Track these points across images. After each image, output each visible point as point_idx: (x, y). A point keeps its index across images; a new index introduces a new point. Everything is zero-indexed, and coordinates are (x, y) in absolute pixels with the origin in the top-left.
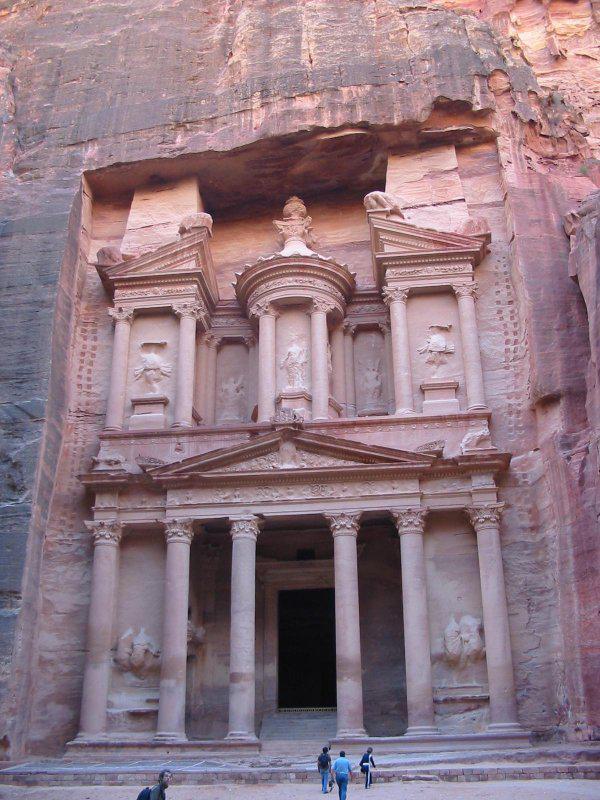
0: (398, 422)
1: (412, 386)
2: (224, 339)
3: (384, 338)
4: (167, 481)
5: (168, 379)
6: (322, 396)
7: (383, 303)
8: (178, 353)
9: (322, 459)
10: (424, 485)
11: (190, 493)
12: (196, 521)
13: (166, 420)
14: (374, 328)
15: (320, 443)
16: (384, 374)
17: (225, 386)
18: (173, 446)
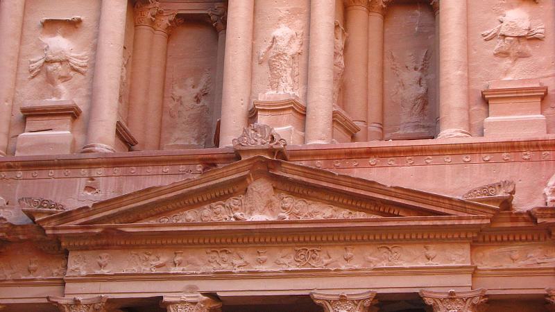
0: (442, 150)
1: (469, 94)
2: (178, 16)
3: (435, 17)
4: (69, 237)
5: (82, 77)
6: (322, 106)
8: (97, 36)
9: (314, 207)
10: (481, 254)
11: (104, 256)
12: (110, 301)
13: (74, 141)
15: (311, 181)
16: (431, 77)
17: (178, 92)
18: (83, 182)
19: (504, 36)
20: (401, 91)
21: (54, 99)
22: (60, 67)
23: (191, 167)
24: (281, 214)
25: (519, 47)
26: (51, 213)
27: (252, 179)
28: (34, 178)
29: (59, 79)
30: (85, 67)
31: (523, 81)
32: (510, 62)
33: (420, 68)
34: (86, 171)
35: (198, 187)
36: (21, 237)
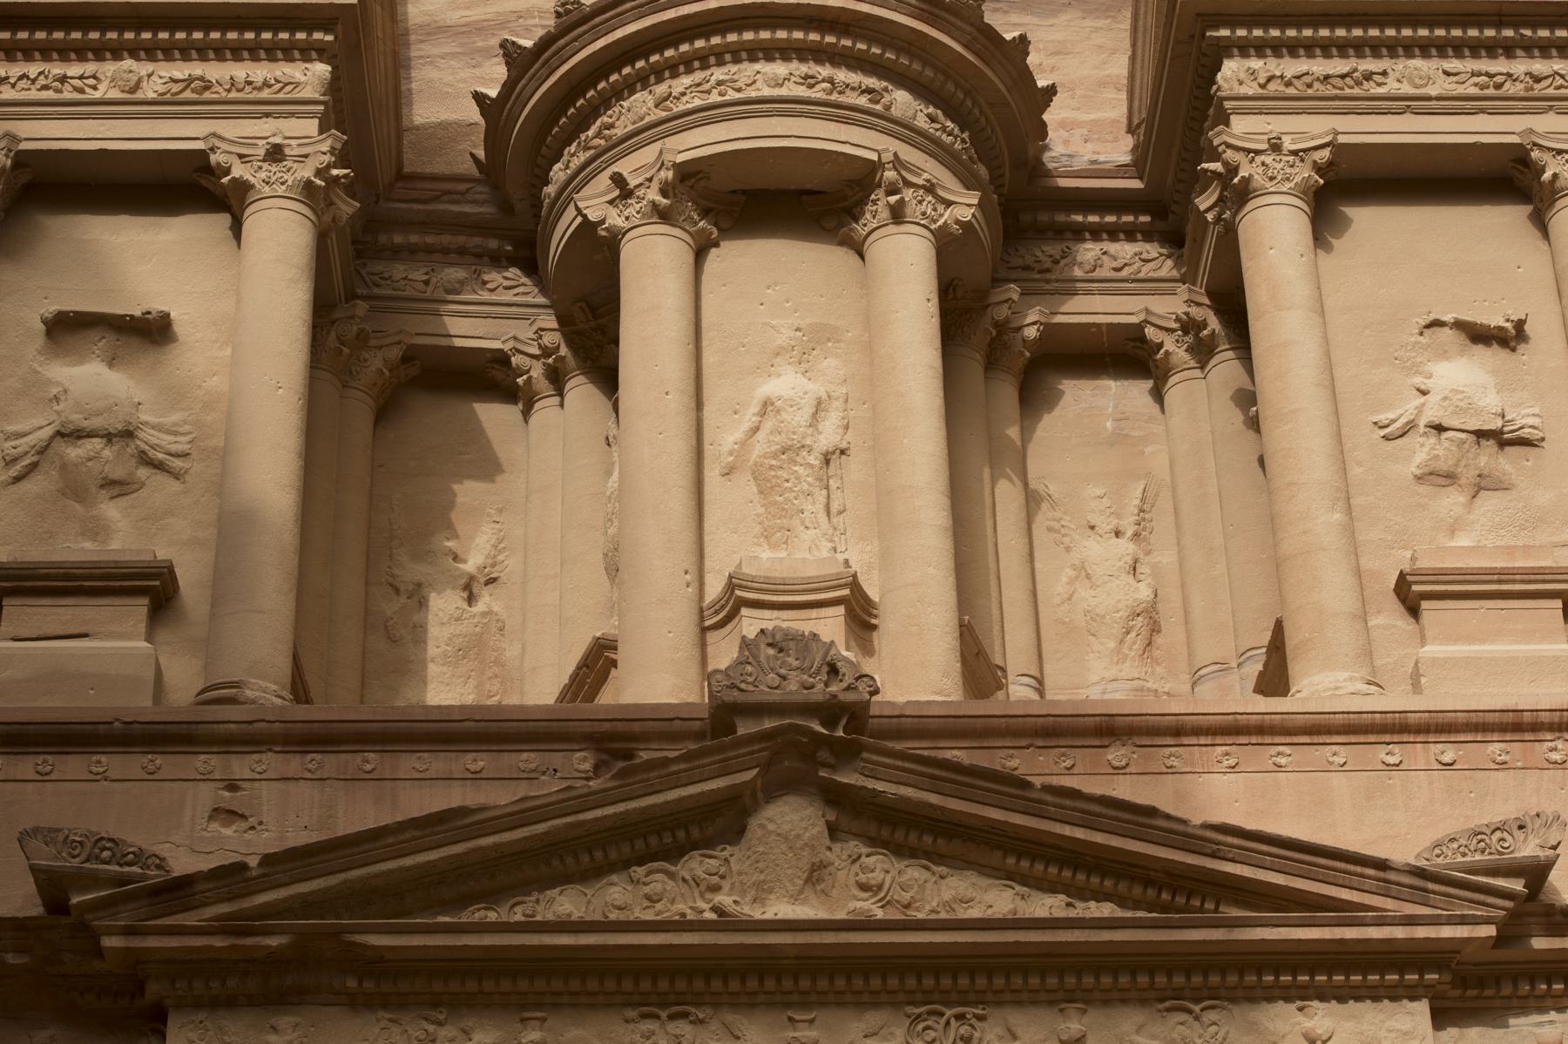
0: (1319, 729)
3: (1158, 395)
5: (174, 486)
7: (1201, 215)
14: (1126, 354)
18: (207, 795)
19: (1440, 428)
20: (1083, 592)
21: (88, 545)
22: (107, 453)
23: (557, 759)
24: (859, 904)
25: (1483, 460)
26: (122, 881)
27: (760, 795)
28: (43, 778)
29: (102, 486)
30: (185, 455)
31: (1511, 551)
32: (1462, 499)
33: (1129, 533)
34: (215, 760)
35: (598, 813)
36: (11, 958)
